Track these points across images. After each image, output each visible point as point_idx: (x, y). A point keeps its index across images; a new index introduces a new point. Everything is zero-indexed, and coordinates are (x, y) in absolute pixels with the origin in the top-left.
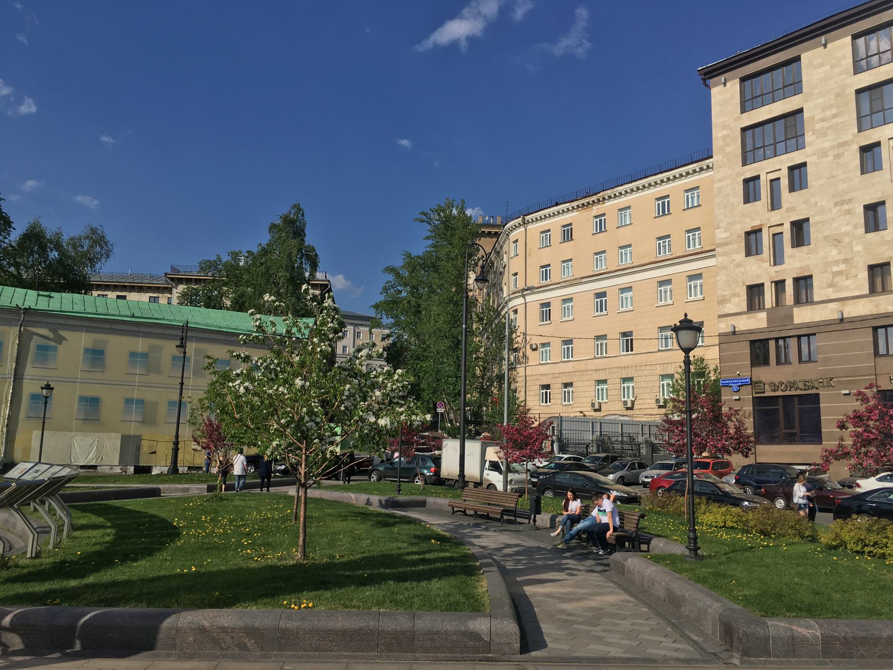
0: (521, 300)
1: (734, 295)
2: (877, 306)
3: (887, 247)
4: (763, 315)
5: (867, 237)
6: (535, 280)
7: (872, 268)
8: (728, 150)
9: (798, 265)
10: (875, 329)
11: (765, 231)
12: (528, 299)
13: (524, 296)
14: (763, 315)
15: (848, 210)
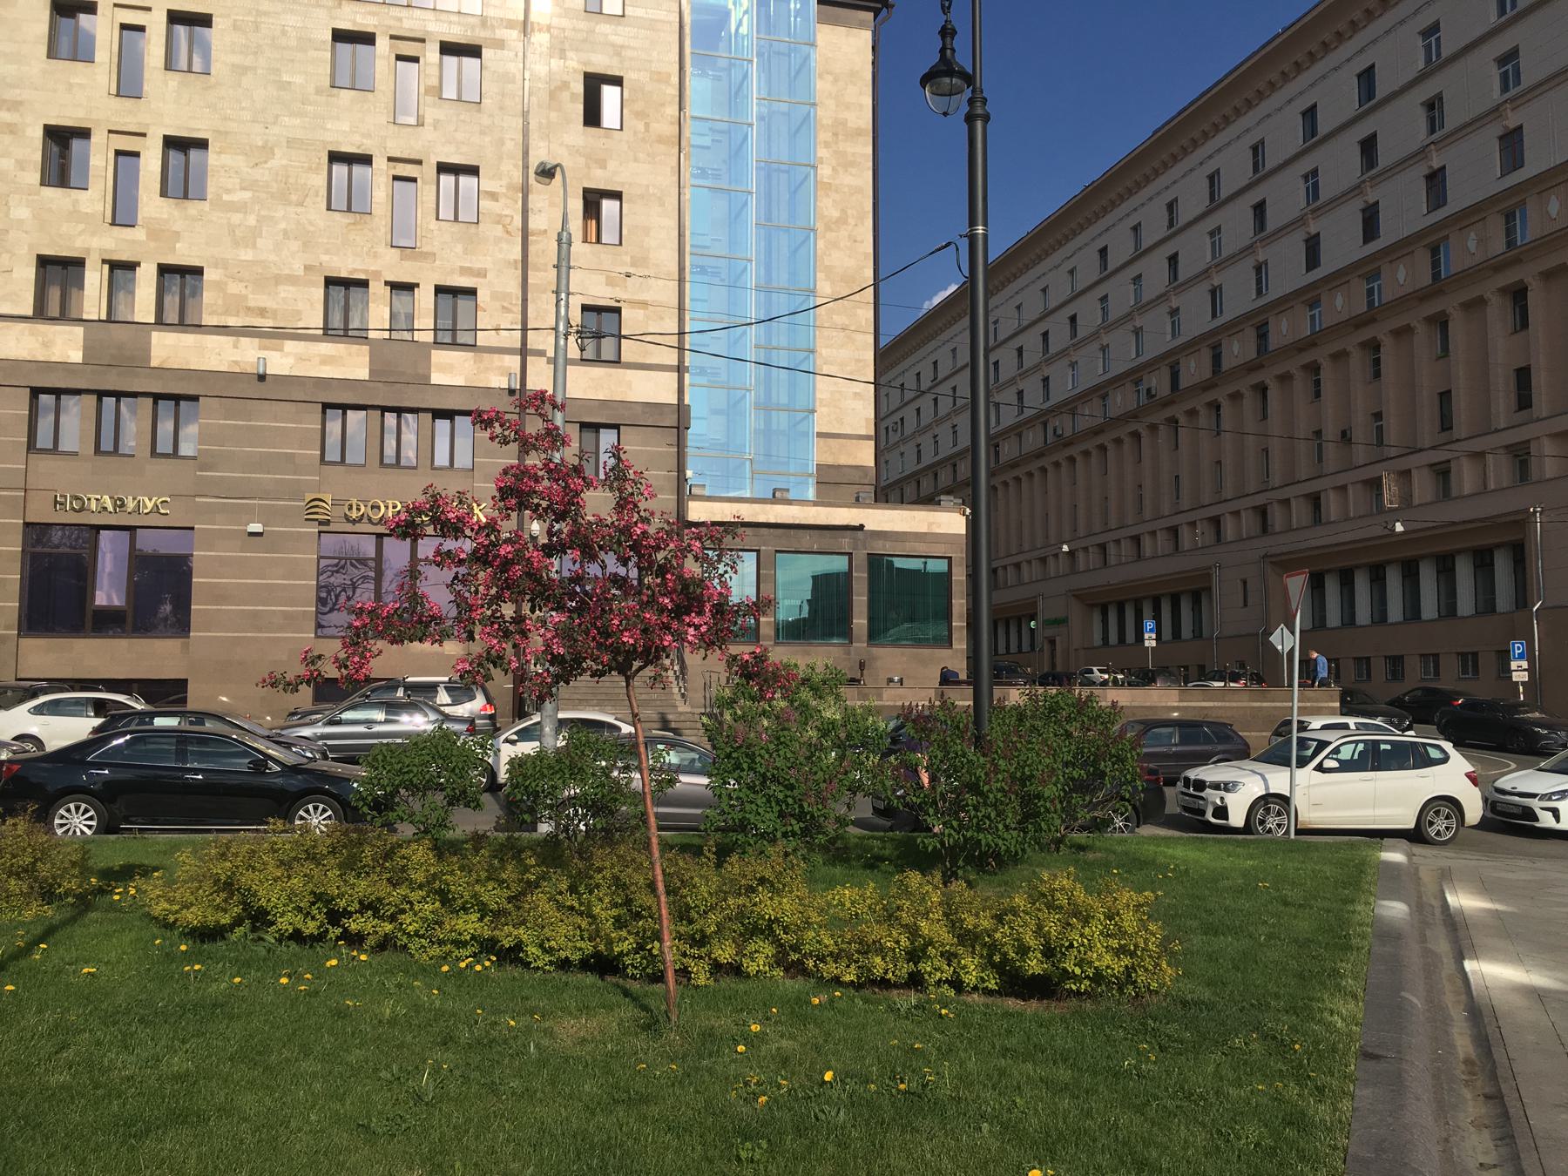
2: (46, 345)
3: (81, 227)
5: (42, 193)
7: (44, 262)
10: (36, 392)
15: (9, 125)
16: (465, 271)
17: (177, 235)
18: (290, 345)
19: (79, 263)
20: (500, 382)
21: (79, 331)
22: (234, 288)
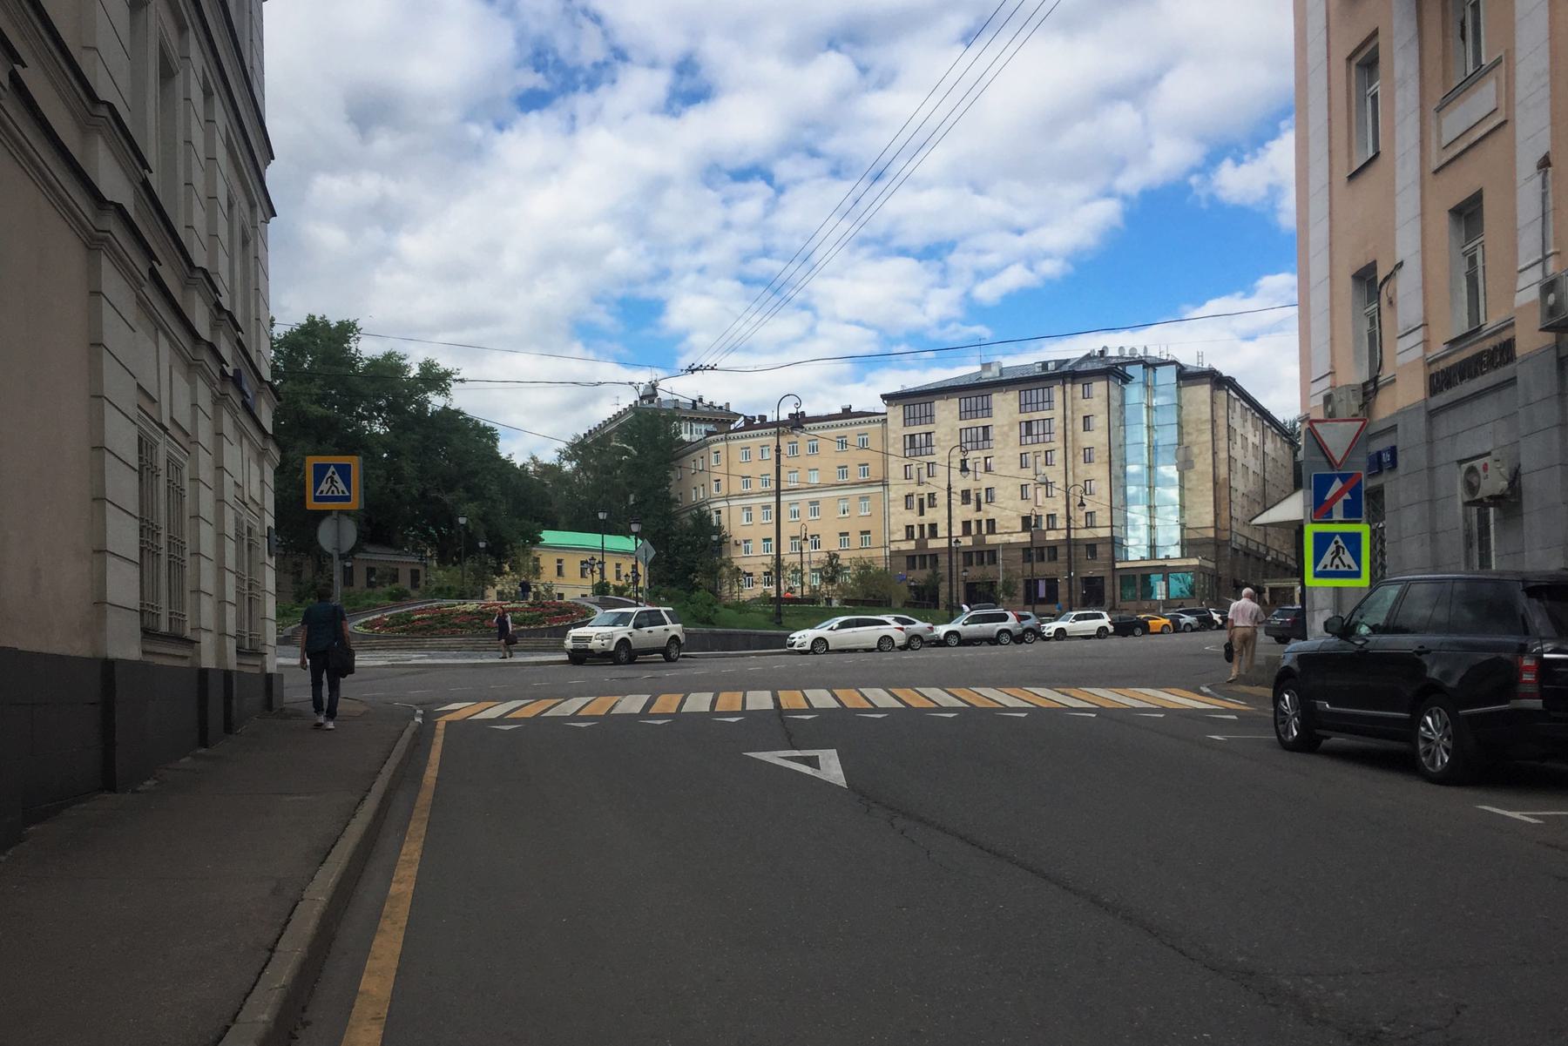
0: (725, 504)
1: (900, 530)
4: (913, 542)
6: (737, 486)
7: (963, 522)
8: (896, 446)
9: (930, 517)
11: (915, 496)
12: (732, 503)
13: (727, 500)
14: (913, 542)
16: (1053, 510)
17: (989, 512)
18: (1014, 535)
19: (970, 522)
20: (1062, 537)
21: (971, 538)
22: (1002, 523)
